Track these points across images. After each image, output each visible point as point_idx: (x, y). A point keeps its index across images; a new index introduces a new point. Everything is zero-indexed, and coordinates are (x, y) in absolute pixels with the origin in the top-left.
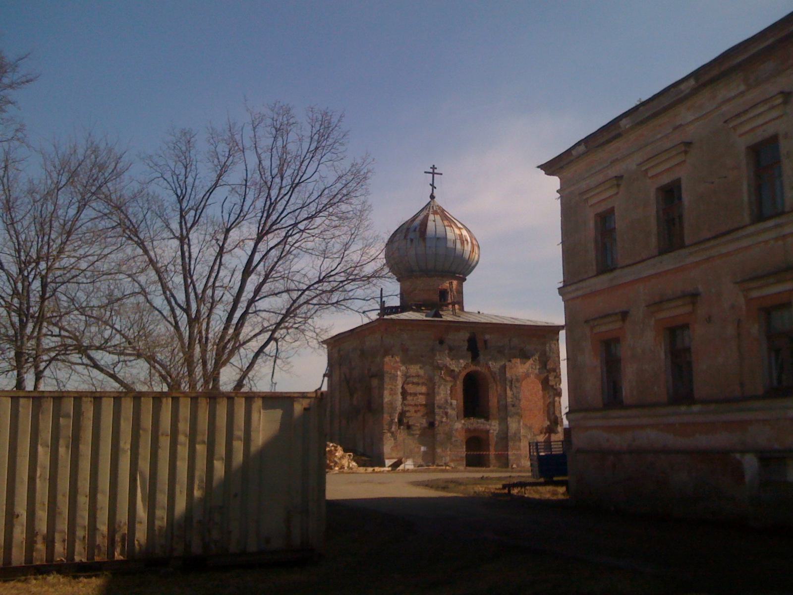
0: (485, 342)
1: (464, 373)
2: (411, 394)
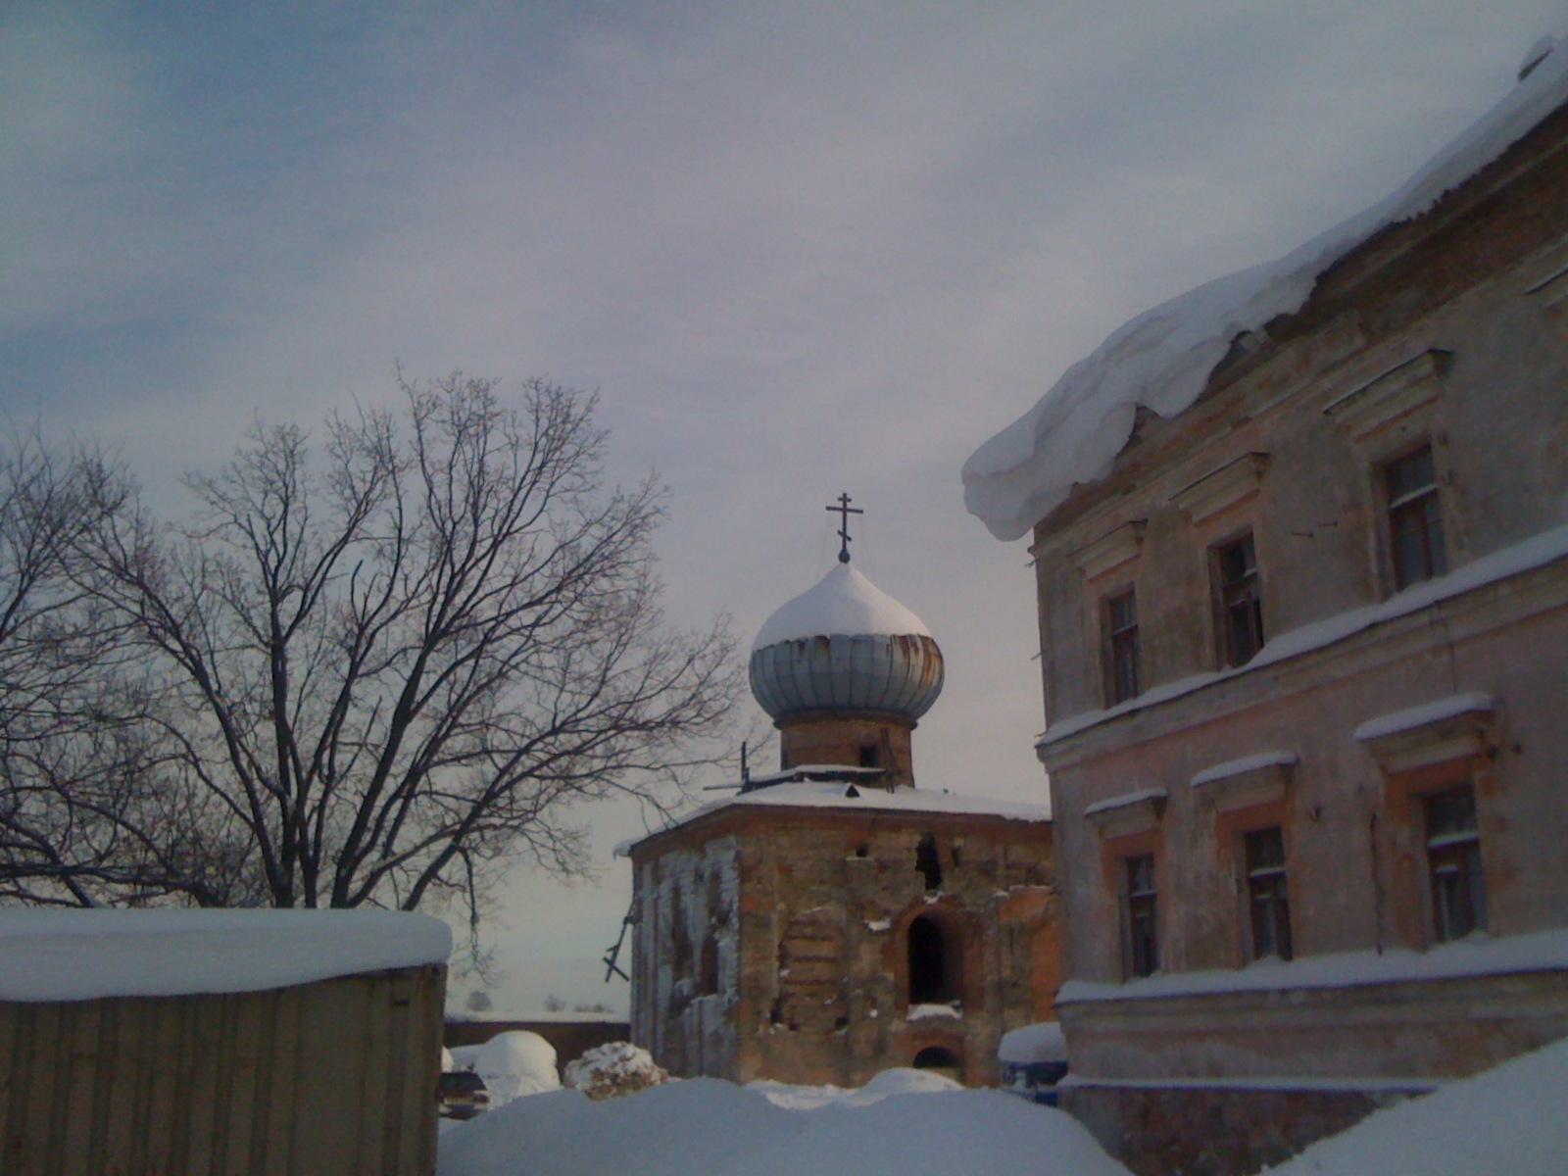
0: (955, 853)
2: (799, 960)
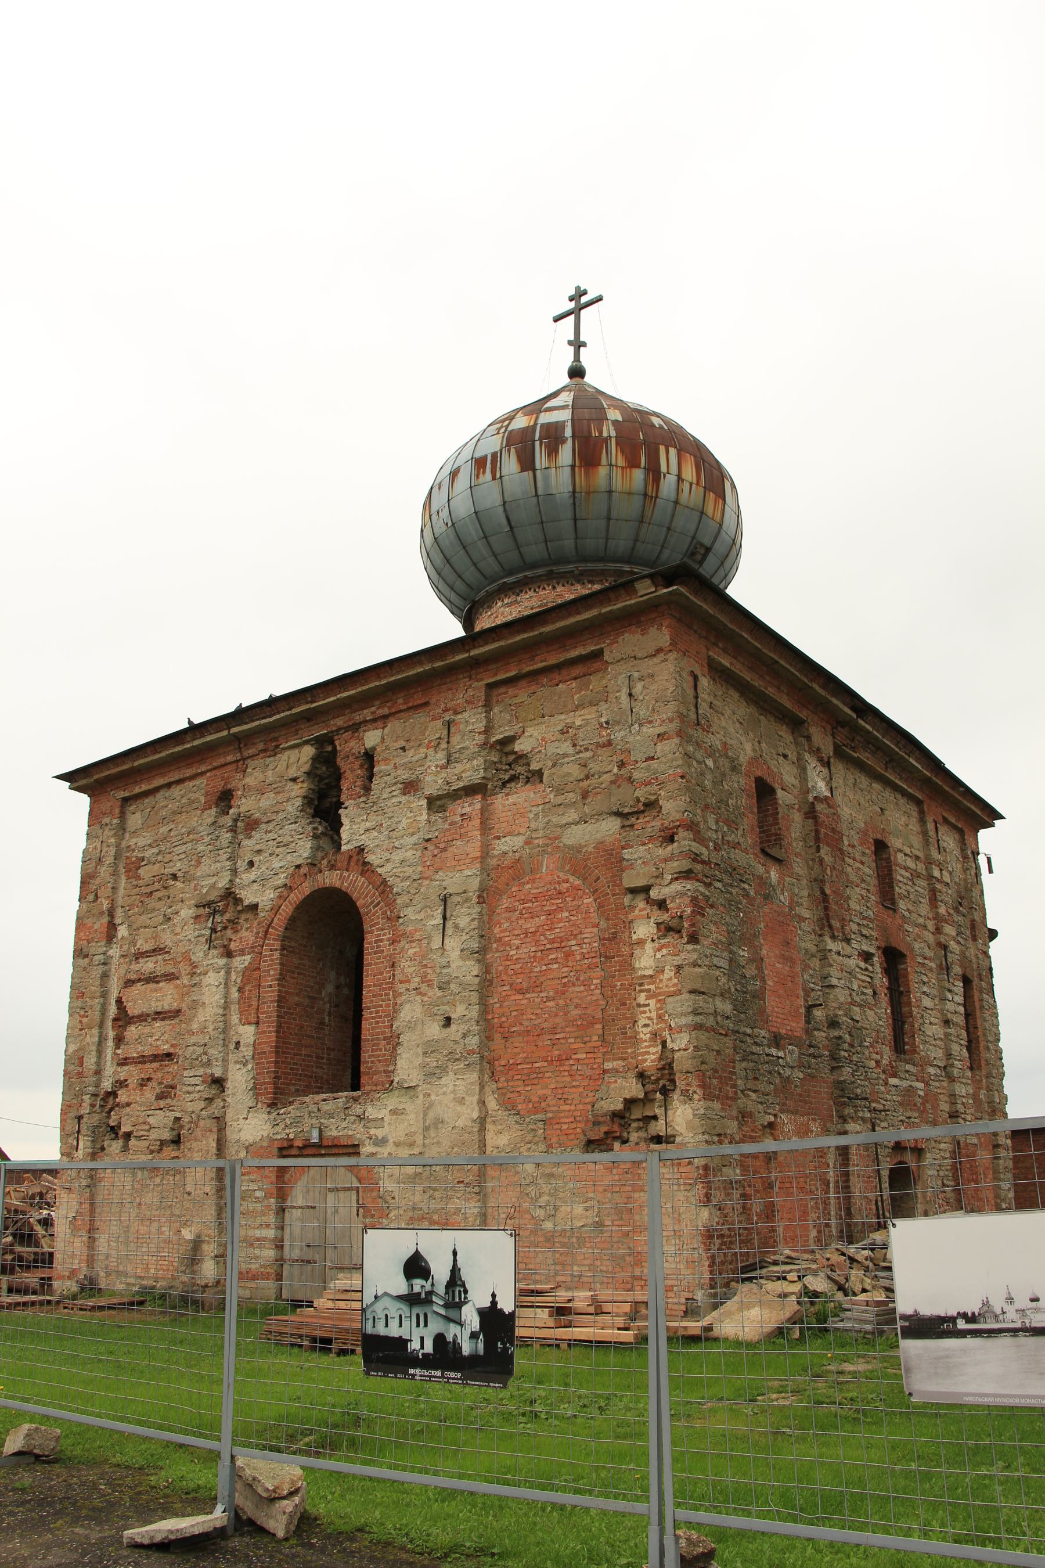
1: (287, 909)
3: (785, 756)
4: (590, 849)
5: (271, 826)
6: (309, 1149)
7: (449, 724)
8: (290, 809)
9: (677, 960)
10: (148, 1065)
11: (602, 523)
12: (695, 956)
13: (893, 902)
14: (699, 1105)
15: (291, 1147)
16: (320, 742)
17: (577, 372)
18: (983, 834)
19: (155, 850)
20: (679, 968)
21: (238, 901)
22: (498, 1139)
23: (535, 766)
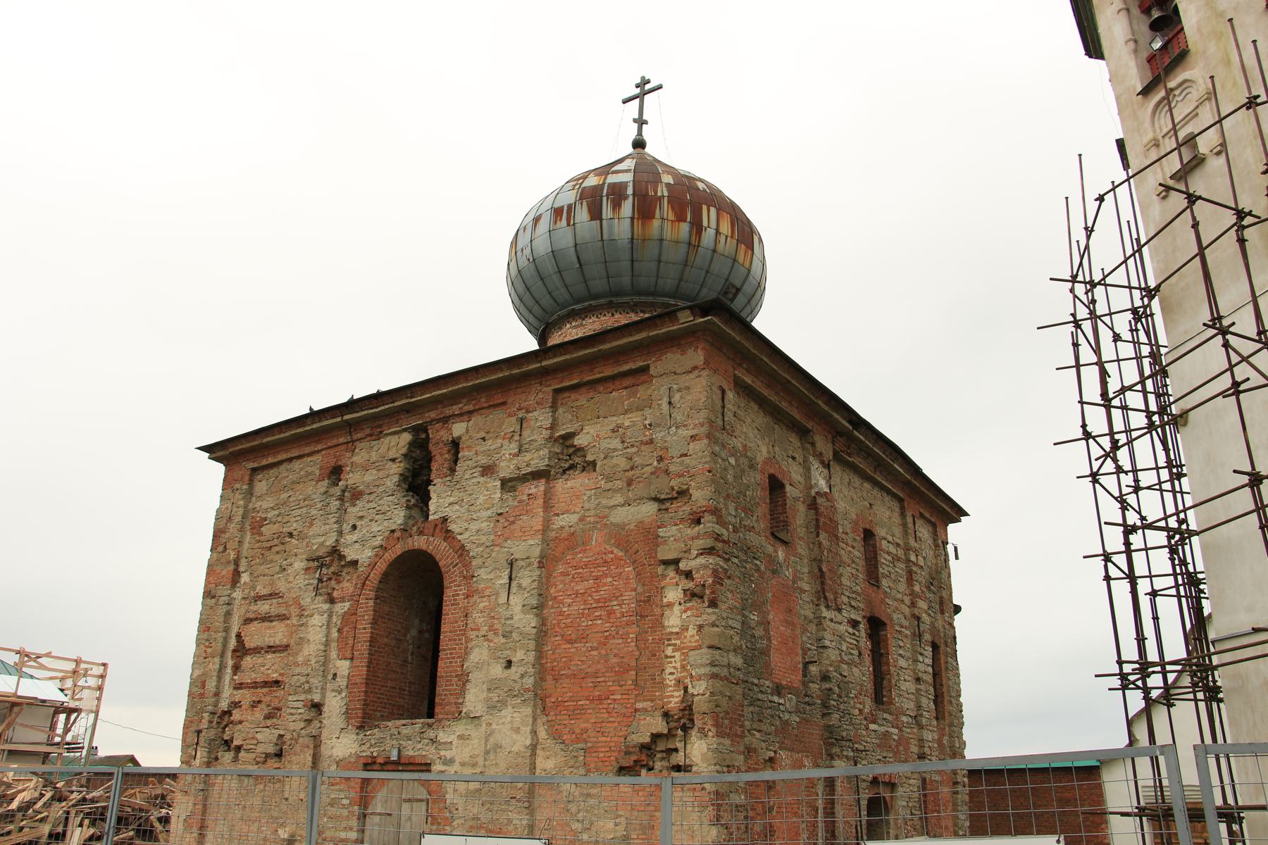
1: (382, 566)
3: (794, 458)
4: (632, 527)
5: (372, 497)
6: (388, 765)
7: (522, 421)
8: (389, 483)
9: (700, 621)
10: (259, 690)
11: (653, 265)
12: (714, 618)
13: (877, 581)
14: (713, 741)
15: (374, 763)
16: (416, 430)
17: (639, 144)
18: (952, 528)
19: (276, 512)
20: (700, 627)
21: (342, 557)
22: (547, 763)
23: (590, 458)
